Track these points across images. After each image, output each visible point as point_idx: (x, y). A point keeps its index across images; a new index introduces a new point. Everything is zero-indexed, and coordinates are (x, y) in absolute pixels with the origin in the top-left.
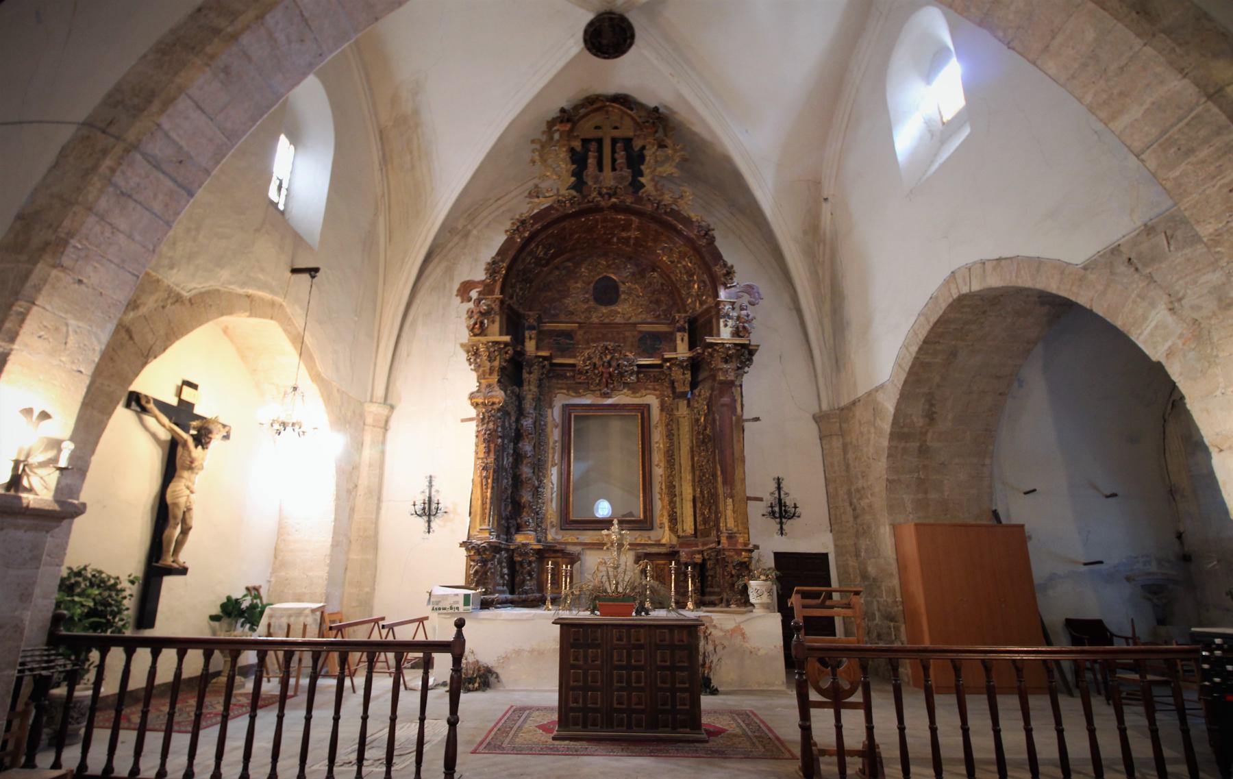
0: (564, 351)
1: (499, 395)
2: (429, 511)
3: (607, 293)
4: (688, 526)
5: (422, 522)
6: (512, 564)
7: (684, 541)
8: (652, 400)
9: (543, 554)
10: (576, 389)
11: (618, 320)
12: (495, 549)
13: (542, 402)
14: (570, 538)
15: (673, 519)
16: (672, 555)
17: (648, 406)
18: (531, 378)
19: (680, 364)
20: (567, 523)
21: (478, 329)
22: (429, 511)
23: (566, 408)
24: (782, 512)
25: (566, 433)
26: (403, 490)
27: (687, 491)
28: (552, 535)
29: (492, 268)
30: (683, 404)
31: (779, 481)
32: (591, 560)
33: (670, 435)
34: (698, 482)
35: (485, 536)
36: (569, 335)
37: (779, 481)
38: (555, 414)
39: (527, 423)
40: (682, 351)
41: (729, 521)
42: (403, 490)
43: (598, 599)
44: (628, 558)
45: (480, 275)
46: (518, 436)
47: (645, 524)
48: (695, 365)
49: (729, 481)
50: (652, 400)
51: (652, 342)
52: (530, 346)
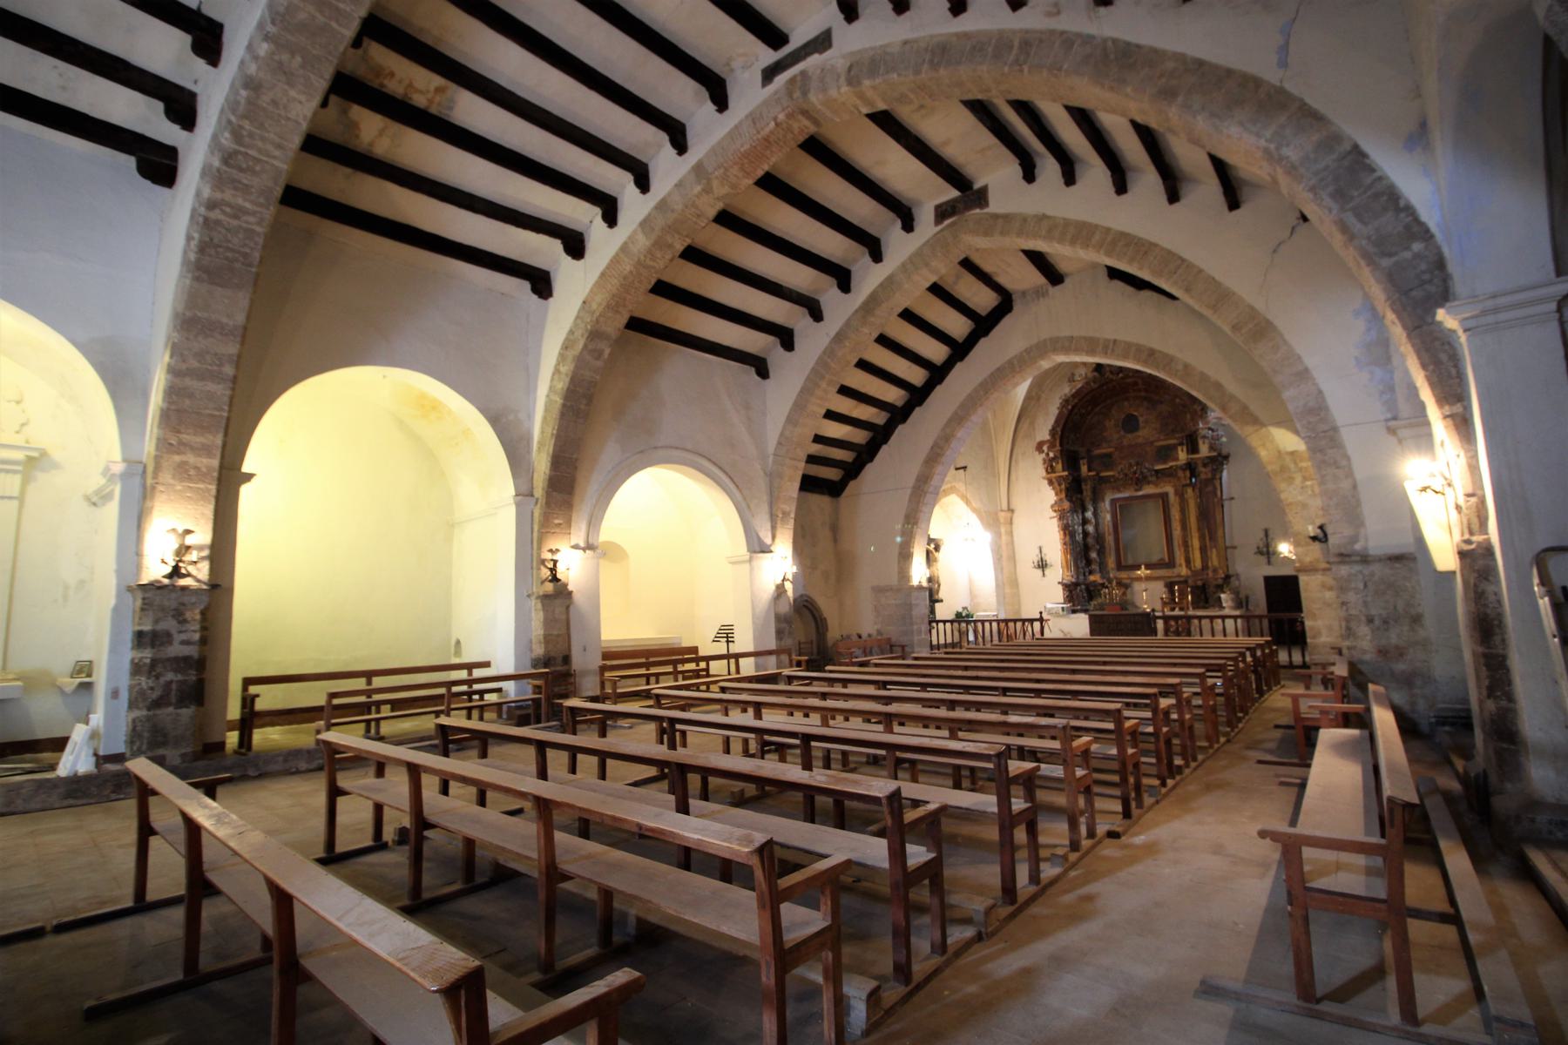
0: (1108, 467)
2: (1042, 565)
3: (1131, 424)
4: (1198, 564)
5: (1039, 572)
6: (1088, 589)
7: (1195, 573)
8: (1170, 489)
11: (1140, 440)
12: (1076, 585)
13: (1097, 498)
14: (1123, 575)
15: (1188, 561)
17: (1167, 494)
18: (1087, 489)
20: (1120, 567)
21: (1050, 468)
22: (1042, 565)
23: (1113, 502)
27: (1196, 543)
29: (1053, 432)
30: (1190, 490)
33: (1183, 511)
34: (1202, 538)
35: (1069, 579)
36: (1109, 455)
38: (1107, 505)
41: (1214, 561)
45: (1048, 437)
47: (1171, 564)
48: (1190, 467)
49: (1213, 538)
50: (1170, 489)
51: (1166, 453)
52: (1084, 469)
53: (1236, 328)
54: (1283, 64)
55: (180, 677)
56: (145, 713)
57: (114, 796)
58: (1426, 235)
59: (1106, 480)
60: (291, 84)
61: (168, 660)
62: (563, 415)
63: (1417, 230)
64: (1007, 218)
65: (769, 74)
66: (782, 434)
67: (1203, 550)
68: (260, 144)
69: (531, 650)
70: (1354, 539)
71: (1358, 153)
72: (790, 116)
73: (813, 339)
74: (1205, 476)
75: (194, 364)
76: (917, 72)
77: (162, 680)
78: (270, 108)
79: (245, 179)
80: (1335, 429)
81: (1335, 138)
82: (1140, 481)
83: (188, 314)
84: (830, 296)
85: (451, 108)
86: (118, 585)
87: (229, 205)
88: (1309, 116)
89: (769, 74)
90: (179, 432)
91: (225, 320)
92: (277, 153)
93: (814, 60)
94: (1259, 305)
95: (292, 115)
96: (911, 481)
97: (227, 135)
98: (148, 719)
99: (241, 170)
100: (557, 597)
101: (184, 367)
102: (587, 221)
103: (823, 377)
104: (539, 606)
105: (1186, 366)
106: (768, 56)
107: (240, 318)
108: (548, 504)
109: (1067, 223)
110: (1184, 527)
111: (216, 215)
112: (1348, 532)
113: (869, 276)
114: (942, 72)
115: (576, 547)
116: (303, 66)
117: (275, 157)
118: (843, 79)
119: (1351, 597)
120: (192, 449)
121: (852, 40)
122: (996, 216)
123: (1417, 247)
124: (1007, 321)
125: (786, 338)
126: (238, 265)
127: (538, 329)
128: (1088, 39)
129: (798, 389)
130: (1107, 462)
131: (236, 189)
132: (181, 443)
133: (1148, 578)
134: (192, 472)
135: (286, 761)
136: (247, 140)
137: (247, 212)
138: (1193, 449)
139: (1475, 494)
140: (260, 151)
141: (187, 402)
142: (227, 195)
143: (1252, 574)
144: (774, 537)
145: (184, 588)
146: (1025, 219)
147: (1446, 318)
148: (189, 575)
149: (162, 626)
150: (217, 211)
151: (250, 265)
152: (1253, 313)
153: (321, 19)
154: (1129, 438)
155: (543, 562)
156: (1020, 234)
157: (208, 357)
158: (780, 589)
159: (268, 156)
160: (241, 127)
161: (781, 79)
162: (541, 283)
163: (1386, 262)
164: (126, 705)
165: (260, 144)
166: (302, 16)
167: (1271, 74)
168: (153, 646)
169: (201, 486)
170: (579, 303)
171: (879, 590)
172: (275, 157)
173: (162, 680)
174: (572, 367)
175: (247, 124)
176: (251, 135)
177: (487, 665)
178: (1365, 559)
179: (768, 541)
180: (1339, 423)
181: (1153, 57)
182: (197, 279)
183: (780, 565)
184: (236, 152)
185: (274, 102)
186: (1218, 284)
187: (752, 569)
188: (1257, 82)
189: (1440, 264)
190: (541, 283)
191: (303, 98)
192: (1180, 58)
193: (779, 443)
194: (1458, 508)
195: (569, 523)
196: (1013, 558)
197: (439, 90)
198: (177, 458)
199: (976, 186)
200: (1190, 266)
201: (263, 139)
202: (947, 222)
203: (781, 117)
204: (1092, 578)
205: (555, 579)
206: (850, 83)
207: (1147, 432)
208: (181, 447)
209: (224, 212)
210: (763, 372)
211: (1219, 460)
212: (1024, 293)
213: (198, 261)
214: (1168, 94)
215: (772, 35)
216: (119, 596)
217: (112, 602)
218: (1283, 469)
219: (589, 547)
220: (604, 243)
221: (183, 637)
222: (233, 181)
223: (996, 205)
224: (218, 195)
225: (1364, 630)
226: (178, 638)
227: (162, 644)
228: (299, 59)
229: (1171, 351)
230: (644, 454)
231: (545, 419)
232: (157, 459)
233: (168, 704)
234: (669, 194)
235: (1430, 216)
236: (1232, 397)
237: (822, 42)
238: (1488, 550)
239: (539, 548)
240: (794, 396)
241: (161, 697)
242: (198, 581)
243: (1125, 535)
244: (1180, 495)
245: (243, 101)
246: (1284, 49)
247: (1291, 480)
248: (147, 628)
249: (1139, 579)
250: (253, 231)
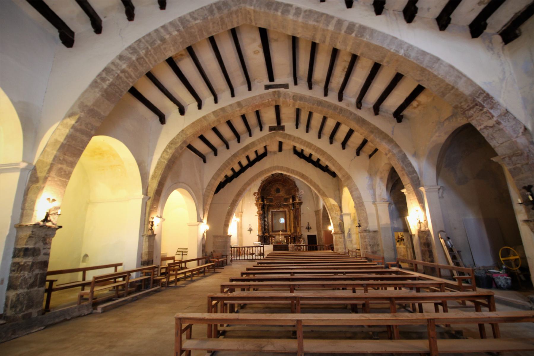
1: (261, 212)
2: (250, 230)
3: (278, 191)
4: (293, 231)
5: (249, 232)
7: (292, 234)
8: (286, 210)
9: (269, 237)
10: (273, 208)
13: (268, 211)
15: (290, 230)
16: (290, 236)
17: (285, 212)
18: (266, 208)
19: (291, 205)
20: (273, 231)
21: (257, 201)
22: (250, 230)
23: (272, 212)
24: (309, 228)
25: (272, 216)
26: (246, 227)
27: (292, 225)
28: (271, 233)
29: (259, 190)
31: (308, 223)
32: (277, 237)
33: (290, 216)
34: (295, 224)
35: (261, 234)
36: (272, 199)
37: (308, 223)
38: (270, 213)
39: (266, 215)
40: (291, 201)
41: (298, 230)
42: (246, 227)
43: (277, 242)
44: (283, 237)
45: (257, 191)
46: (264, 217)
47: (286, 231)
48: (293, 205)
49: (298, 224)
50: (286, 210)
51: (286, 200)
52: (265, 202)
53: (343, 176)
54: (393, 134)
55: (41, 272)
56: (26, 290)
57: (13, 336)
58: (416, 173)
59: (269, 206)
60: (173, 46)
61: (39, 262)
62: (166, 167)
63: (414, 171)
64: (290, 136)
65: (267, 87)
66: (210, 182)
67: (295, 227)
68: (151, 58)
69: (142, 258)
70: (367, 227)
71: (405, 155)
72: (272, 100)
73: (225, 155)
74: (296, 207)
75: (83, 127)
76: (313, 105)
77: (34, 273)
79: (139, 67)
80: (363, 202)
81: (401, 151)
82: (279, 207)
83: (92, 107)
84: (233, 143)
85: (180, 61)
86: (11, 224)
87: (128, 74)
88: (397, 146)
89: (267, 87)
90: (65, 155)
91: (102, 113)
92: (153, 63)
93: (282, 90)
94: (349, 172)
95: (166, 54)
96: (230, 201)
97: (144, 51)
98: (27, 293)
99: (140, 64)
100: (152, 236)
101: (79, 127)
102: (188, 104)
103: (227, 166)
104: (147, 240)
105: (311, 180)
106: (268, 83)
107: (107, 113)
108: (154, 199)
109: (306, 142)
110: (290, 221)
111: (122, 75)
112: (366, 225)
113: (247, 141)
114: (320, 107)
115: (157, 217)
116: (181, 43)
117: (151, 64)
118: (291, 98)
119: (367, 240)
120: (67, 163)
121: (293, 89)
122: (287, 134)
123: (415, 174)
124: (265, 159)
125: (215, 151)
126: (117, 94)
127: (158, 134)
128: (355, 114)
129: (217, 169)
130: (271, 200)
131: (134, 69)
132: (64, 160)
133: (282, 235)
134: (63, 173)
135: (79, 311)
136: (148, 55)
137: (131, 77)
138: (294, 199)
139: (426, 220)
140: (149, 60)
141: (74, 142)
142: (130, 71)
143: (305, 234)
144: (203, 217)
145: (50, 227)
146: (295, 137)
147: (422, 189)
148: (50, 221)
149: (37, 246)
150: (123, 74)
151: (121, 96)
152: (347, 173)
153: (197, 33)
154: (277, 195)
155: (149, 222)
156: (293, 141)
157: (89, 126)
158: (204, 234)
160: (150, 51)
161: (271, 90)
162: (162, 120)
163: (410, 176)
164: (6, 288)
165: (151, 58)
166: (193, 30)
167: (391, 136)
168: (33, 256)
169: (64, 180)
170: (180, 130)
171: (215, 237)
172: (151, 64)
173: (34, 273)
174: (174, 151)
175: (152, 51)
176: (150, 55)
177: (121, 264)
178: (369, 232)
179: (202, 218)
180: (364, 201)
181: (368, 124)
182: (102, 95)
183: (204, 227)
184: (142, 58)
185: (165, 49)
186: (340, 165)
187: (198, 229)
188: (388, 136)
189: (418, 178)
190: (162, 120)
191: (173, 51)
192: (374, 126)
193: (208, 185)
194: (420, 223)
195: (157, 207)
196: (241, 227)
197: (182, 55)
198: (60, 166)
199: (282, 124)
200: (334, 160)
201: (153, 57)
202: (272, 132)
203: (270, 100)
204: (266, 234)
205: (152, 229)
206: (293, 99)
207: (282, 194)
208: (61, 162)
209: (125, 75)
210: (205, 161)
211: (300, 203)
212: (270, 152)
213: (107, 89)
214: (372, 132)
215: (271, 79)
216: (11, 230)
217: (7, 233)
218: (332, 208)
219: (161, 217)
220: (193, 113)
221: (44, 251)
222: (135, 66)
223: (287, 131)
224: (127, 69)
225: (369, 247)
226: (43, 252)
227: (37, 255)
228: (181, 40)
229: (308, 176)
230: (176, 185)
231: (157, 168)
232: (52, 165)
233: (36, 286)
234: (226, 107)
235: (417, 169)
236: (321, 189)
237: (286, 86)
238: (429, 231)
239: (149, 217)
240: (216, 171)
241: (33, 283)
242: (53, 224)
243: (274, 222)
244: (289, 211)
245: (157, 44)
246: (393, 131)
247: (333, 211)
248: (30, 246)
249: (279, 235)
250: (129, 84)
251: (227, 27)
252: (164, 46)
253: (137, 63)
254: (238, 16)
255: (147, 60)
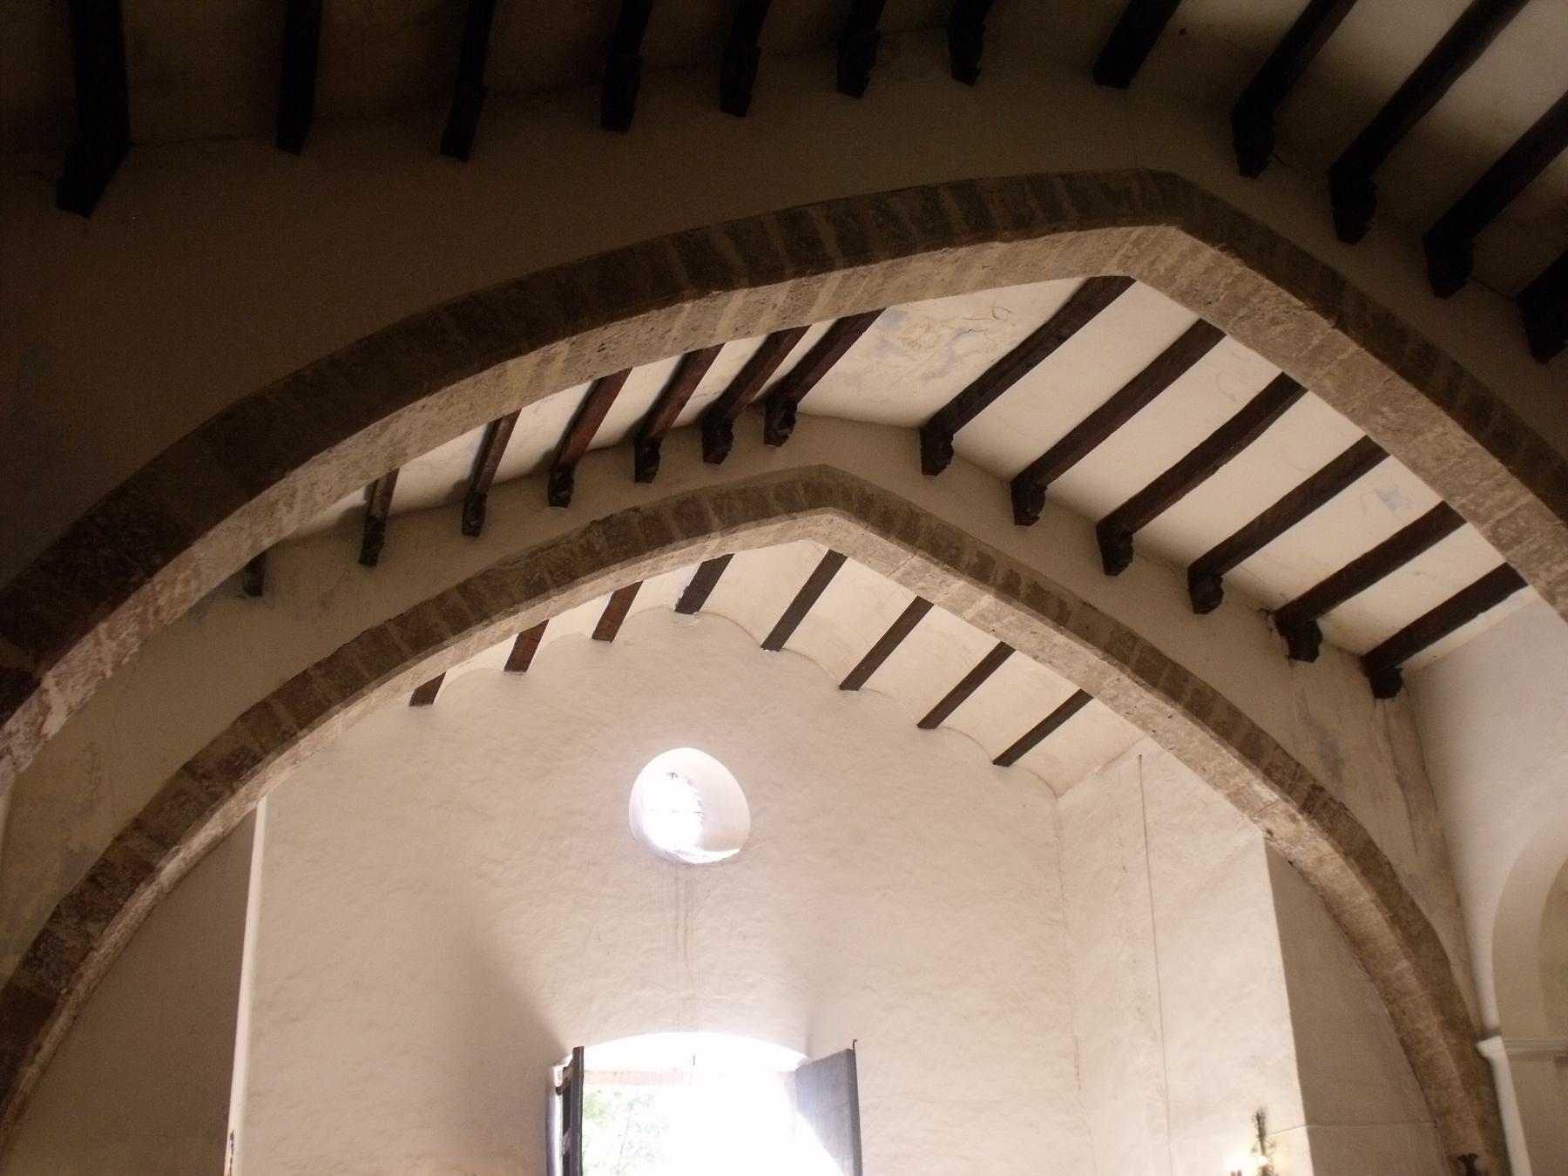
60: (1417, 432)
68: (1489, 503)
78: (1445, 467)
92: (1508, 493)
116: (1396, 411)
131: (1540, 562)
136: (1480, 510)
150: (1560, 599)
159: (1511, 503)
165: (1489, 503)
184: (1494, 529)
228: (1385, 409)
251: (1241, 277)
252: (1430, 464)
253: (1517, 548)
254: (1174, 269)
255: (1500, 515)
